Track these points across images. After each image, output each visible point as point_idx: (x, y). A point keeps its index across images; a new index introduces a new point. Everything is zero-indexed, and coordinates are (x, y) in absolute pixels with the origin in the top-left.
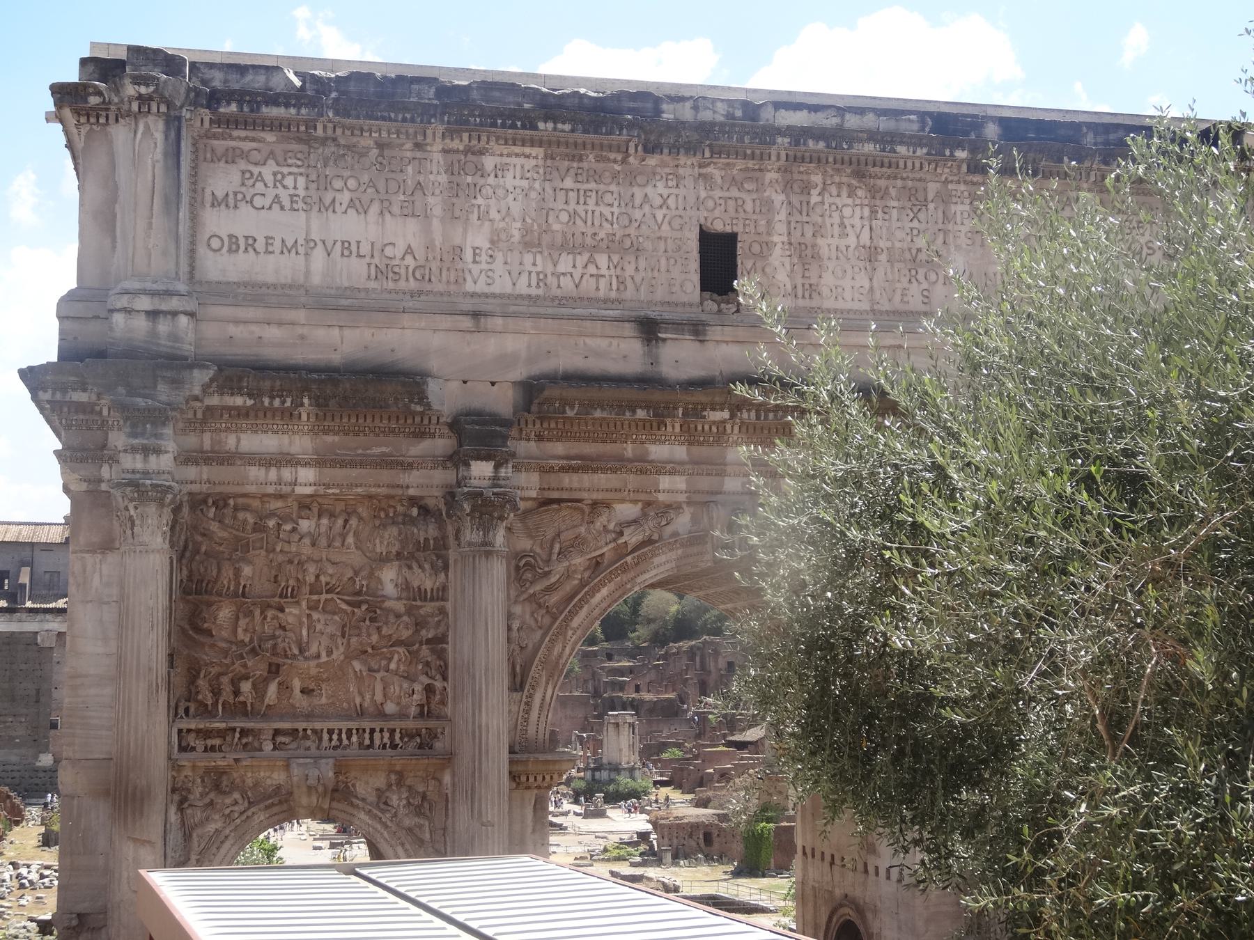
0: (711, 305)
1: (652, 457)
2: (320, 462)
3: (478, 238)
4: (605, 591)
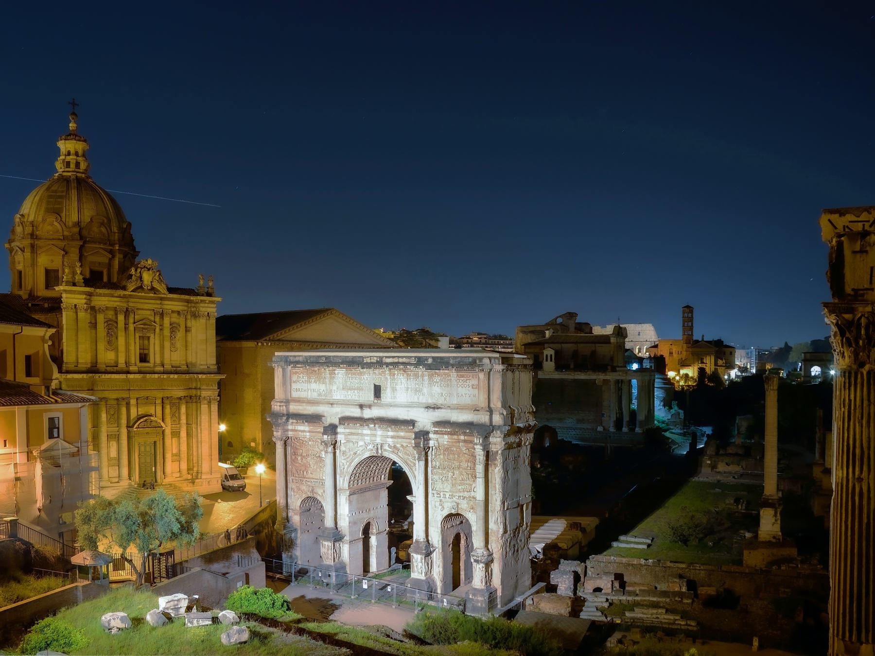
0: (376, 401)
1: (364, 433)
2: (309, 432)
3: (335, 388)
4: (357, 459)
